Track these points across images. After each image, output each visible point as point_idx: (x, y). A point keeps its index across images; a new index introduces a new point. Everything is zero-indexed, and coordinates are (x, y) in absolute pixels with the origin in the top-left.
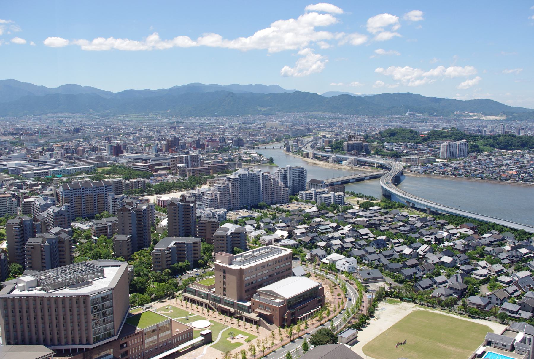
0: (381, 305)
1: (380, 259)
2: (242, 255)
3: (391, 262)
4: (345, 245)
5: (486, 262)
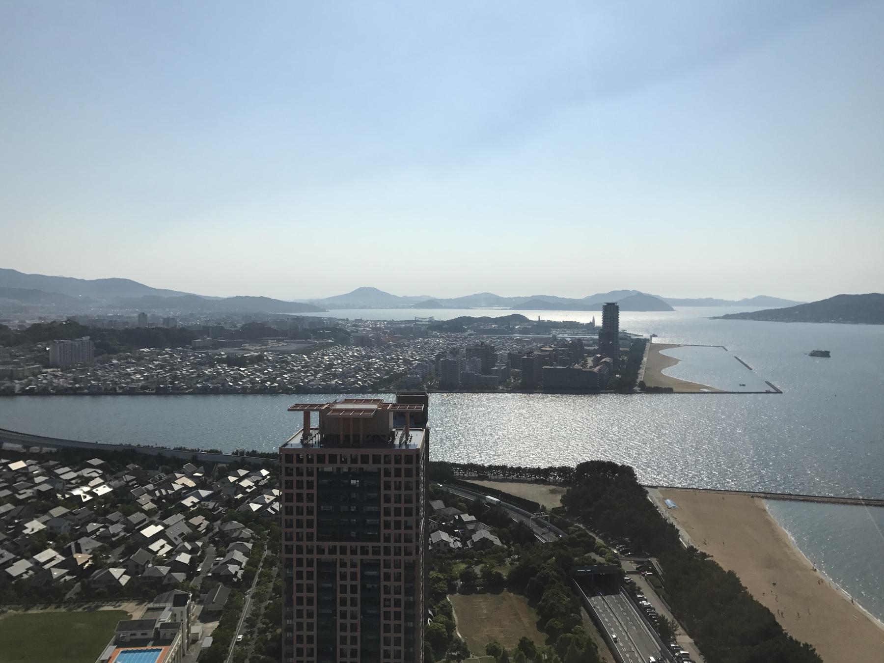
5: (120, 514)
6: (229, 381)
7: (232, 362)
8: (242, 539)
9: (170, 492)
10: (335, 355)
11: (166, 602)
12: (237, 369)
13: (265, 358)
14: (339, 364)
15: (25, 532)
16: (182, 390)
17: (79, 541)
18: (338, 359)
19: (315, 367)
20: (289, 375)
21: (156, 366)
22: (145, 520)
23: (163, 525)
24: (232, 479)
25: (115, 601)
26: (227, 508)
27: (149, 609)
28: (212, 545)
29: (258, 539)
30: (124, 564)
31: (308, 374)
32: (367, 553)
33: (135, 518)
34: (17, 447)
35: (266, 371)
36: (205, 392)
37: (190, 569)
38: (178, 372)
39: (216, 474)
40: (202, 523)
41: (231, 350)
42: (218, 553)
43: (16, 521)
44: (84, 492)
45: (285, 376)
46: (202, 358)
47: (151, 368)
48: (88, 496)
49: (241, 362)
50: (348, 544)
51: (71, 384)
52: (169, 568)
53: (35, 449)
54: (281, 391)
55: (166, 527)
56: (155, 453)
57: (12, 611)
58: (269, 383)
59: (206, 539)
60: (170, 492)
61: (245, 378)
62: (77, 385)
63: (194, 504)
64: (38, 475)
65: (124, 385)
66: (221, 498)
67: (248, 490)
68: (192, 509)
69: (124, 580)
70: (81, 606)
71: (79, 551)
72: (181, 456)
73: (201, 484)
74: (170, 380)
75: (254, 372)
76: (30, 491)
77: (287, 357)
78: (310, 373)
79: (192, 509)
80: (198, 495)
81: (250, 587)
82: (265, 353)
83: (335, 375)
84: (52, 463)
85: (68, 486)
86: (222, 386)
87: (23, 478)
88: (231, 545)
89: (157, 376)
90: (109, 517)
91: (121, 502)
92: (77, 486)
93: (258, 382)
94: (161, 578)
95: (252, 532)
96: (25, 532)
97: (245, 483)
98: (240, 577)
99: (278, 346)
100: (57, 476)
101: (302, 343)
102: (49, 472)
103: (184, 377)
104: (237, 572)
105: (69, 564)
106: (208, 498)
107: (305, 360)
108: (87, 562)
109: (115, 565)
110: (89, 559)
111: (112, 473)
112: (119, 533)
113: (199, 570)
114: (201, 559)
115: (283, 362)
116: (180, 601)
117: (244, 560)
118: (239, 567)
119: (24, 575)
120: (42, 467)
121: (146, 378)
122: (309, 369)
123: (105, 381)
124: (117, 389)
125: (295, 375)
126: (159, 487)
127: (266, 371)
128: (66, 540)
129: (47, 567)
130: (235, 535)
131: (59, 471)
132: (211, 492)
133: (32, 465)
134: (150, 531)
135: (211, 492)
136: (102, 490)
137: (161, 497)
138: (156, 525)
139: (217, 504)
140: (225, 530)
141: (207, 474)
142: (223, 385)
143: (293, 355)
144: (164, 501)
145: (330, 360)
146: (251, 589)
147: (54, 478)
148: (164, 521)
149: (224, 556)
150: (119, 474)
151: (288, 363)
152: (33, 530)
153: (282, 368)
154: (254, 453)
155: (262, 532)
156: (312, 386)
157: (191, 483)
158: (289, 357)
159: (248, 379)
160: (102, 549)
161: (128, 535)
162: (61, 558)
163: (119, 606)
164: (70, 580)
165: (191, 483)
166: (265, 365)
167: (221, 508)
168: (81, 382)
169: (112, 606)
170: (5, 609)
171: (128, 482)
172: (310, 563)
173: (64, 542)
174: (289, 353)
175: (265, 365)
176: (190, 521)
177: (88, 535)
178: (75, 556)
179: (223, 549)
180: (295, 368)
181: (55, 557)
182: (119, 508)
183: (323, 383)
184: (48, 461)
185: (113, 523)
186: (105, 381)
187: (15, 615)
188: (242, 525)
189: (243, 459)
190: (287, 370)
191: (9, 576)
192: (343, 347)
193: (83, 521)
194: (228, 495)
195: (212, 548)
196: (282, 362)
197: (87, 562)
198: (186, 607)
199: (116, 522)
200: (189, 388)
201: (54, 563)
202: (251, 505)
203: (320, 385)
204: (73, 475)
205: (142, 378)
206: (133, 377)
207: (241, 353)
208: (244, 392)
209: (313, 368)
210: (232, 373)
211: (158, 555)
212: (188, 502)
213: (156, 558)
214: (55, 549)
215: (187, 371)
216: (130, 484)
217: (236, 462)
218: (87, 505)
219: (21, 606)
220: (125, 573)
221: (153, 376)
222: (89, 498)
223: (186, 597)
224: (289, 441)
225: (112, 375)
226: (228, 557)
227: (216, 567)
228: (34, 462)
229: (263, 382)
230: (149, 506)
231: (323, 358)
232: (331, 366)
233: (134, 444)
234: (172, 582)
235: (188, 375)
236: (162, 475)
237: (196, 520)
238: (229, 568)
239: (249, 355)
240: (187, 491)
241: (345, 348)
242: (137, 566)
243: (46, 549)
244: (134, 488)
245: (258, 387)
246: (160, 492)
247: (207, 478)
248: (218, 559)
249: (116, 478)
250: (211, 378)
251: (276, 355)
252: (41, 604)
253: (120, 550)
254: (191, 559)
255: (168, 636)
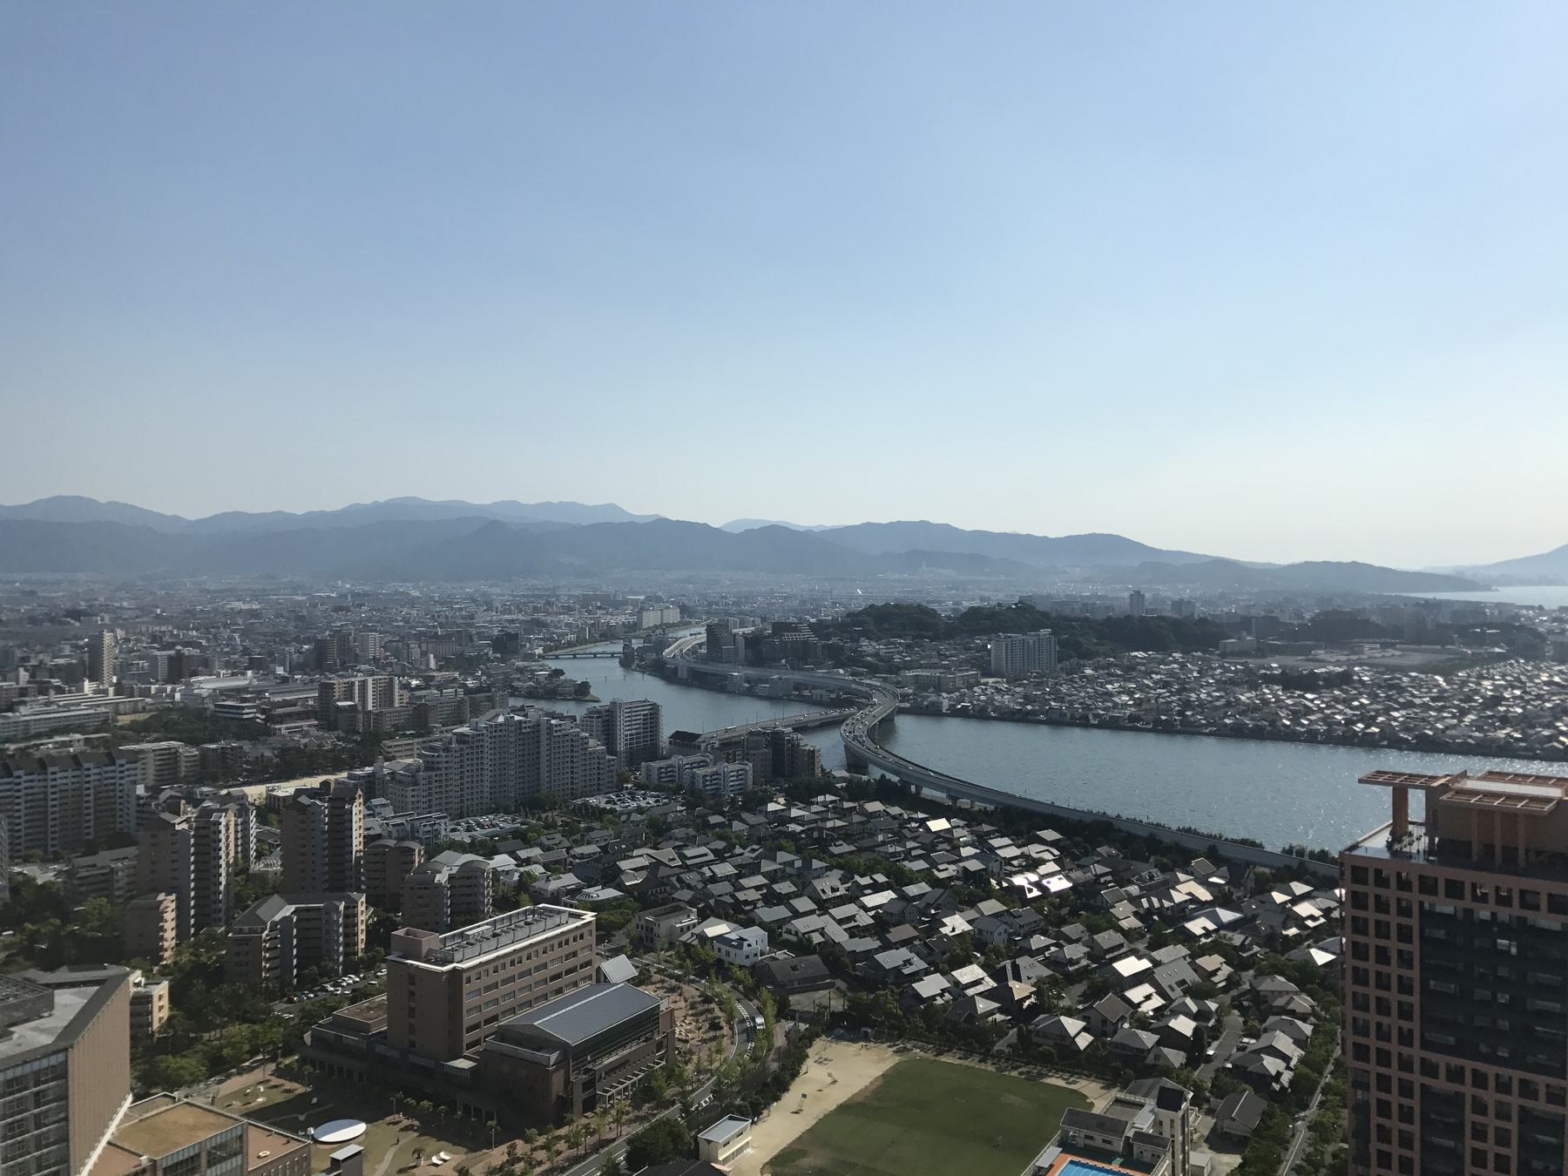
0: (819, 1046)
1: (823, 928)
2: (463, 932)
3: (852, 936)
4: (741, 896)
5: (1082, 928)
6: (1284, 717)
7: (1291, 681)
8: (1293, 1013)
9: (1167, 904)
10: (1509, 678)
11: (1146, 1096)
12: (1299, 696)
13: (1355, 678)
14: (1515, 698)
15: (944, 930)
16: (1198, 726)
17: (1018, 961)
18: (1514, 688)
19: (1460, 700)
20: (1404, 712)
21: (1155, 683)
22: (1121, 946)
23: (1152, 960)
24: (1279, 897)
25: (1069, 1072)
26: (1267, 950)
27: (1117, 1101)
28: (1236, 1012)
29: (1326, 1019)
30: (1084, 1014)
31: (1445, 715)
32: (1535, 1096)
33: (1107, 939)
34: (939, 796)
35: (1356, 703)
36: (1238, 733)
37: (1193, 1048)
38: (1193, 695)
39: (1251, 884)
40: (1219, 969)
41: (1290, 661)
42: (1246, 1030)
43: (933, 912)
44: (1030, 883)
45: (1395, 714)
46: (1236, 672)
47: (1148, 686)
48: (1035, 889)
49: (1309, 683)
50: (1491, 1070)
51: (1020, 704)
52: (1156, 1037)
53: (964, 803)
54: (1385, 743)
55: (1156, 963)
56: (1144, 833)
57: (918, 1050)
58: (1361, 725)
59: (1227, 999)
60: (1167, 904)
61: (1313, 712)
62: (1029, 707)
63: (1208, 933)
64: (966, 845)
65: (1102, 712)
66: (1257, 928)
67: (1310, 923)
68: (1203, 940)
69: (1083, 1041)
70: (1017, 1068)
71: (1017, 978)
72: (1191, 843)
73: (1223, 899)
74: (1177, 708)
75: (1333, 703)
76: (952, 867)
77: (1400, 679)
78: (1449, 712)
79: (1203, 940)
80: (1214, 918)
81: (1306, 1107)
82: (1356, 669)
83: (1505, 720)
84: (986, 828)
85: (1008, 868)
86: (1270, 725)
87: (946, 846)
88: (1272, 1019)
89: (1156, 700)
90: (1066, 929)
91: (1087, 908)
92: (1022, 870)
93: (1339, 723)
94: (1142, 1052)
95: (1314, 1003)
96: (944, 930)
97: (1304, 909)
98: (1286, 1085)
99: (1383, 657)
100: (992, 849)
101: (1434, 652)
102: (981, 841)
103: (1202, 704)
104: (1279, 1074)
105: (1001, 994)
106: (1232, 926)
107: (1438, 686)
108: (1028, 997)
109: (1070, 1013)
110: (1031, 993)
111: (1075, 858)
112: (1080, 958)
113: (1211, 1052)
114: (1215, 1033)
115: (1391, 687)
116: (1169, 1100)
117: (1296, 1054)
118: (1284, 1065)
119: (938, 998)
120: (972, 833)
121: (1138, 703)
122: (1447, 704)
123: (1071, 703)
124: (1091, 717)
125: (1416, 713)
126: (1148, 891)
127: (1356, 703)
128: (1000, 956)
129: (970, 992)
130: (1280, 1002)
131: (996, 842)
132: (1238, 915)
133: (958, 827)
134: (1128, 966)
135: (1238, 915)
136: (1058, 884)
137: (1151, 911)
138: (1139, 958)
139: (1250, 939)
140: (1260, 988)
141: (1233, 880)
142: (1272, 723)
143: (1413, 674)
144: (1156, 917)
145: (1496, 688)
146: (1307, 1113)
147: (987, 852)
148: (1155, 954)
149: (1257, 1036)
150: (1084, 861)
151: (1401, 690)
152: (954, 930)
153: (1389, 698)
154: (1323, 856)
155: (1332, 1008)
156: (1453, 737)
157: (1204, 895)
158: (1405, 679)
159: (1320, 715)
160: (1052, 981)
161: (1094, 966)
162: (990, 983)
163: (1075, 1082)
164: (1004, 1021)
165: (1204, 895)
166: (1354, 692)
167: (1256, 949)
168: (1035, 701)
169: (1064, 1079)
170: (909, 1046)
171: (1098, 877)
172: (1406, 1090)
173: (998, 958)
174: (1404, 671)
175: (1354, 692)
176: (1198, 961)
177: (1032, 953)
178: (1013, 984)
179: (1256, 1023)
180: (1417, 701)
181: (983, 979)
182: (1082, 918)
183: (1477, 734)
184: (980, 824)
185: (1070, 941)
186: (1071, 703)
187: (922, 1059)
188: (1293, 987)
189: (1302, 864)
190: (1399, 703)
191: (917, 995)
192: (1527, 662)
193: (1026, 929)
194: (1272, 927)
195: (1235, 1017)
196: (1389, 688)
197: (1028, 997)
198: (1180, 1113)
199: (1077, 941)
200: (1209, 725)
201: (980, 988)
202: (1313, 951)
203: (1471, 737)
204: (1013, 852)
205: (1131, 702)
206: (1115, 699)
207: (1310, 666)
208: (1311, 738)
209: (1456, 702)
210: (1289, 702)
211: (1140, 1010)
212: (1197, 926)
213: (1136, 1016)
214: (982, 967)
215: (1209, 694)
216: (1102, 880)
217: (1288, 868)
218: (1034, 905)
219: (931, 1046)
220: (1085, 1029)
221: (1149, 700)
222: (1036, 893)
223: (1180, 1097)
224: (1365, 839)
225: (1082, 694)
226: (1263, 1042)
227: (1241, 1054)
228: (962, 823)
229: (1350, 722)
230: (1130, 923)
231: (1479, 684)
232: (1497, 700)
233: (1112, 812)
234: (1160, 1062)
235: (1211, 702)
236: (1155, 871)
237: (1210, 962)
238: (1265, 1062)
239: (1324, 670)
240: (1195, 907)
241: (1533, 666)
242: (1105, 1021)
243: (971, 963)
244: (1108, 888)
245: (1340, 733)
246: (1150, 902)
247: (1232, 889)
248: (1245, 1040)
249: (1080, 867)
250: (1250, 709)
251: (1377, 672)
252: (959, 1049)
253: (1080, 988)
254: (1196, 1030)
255: (1147, 1157)
